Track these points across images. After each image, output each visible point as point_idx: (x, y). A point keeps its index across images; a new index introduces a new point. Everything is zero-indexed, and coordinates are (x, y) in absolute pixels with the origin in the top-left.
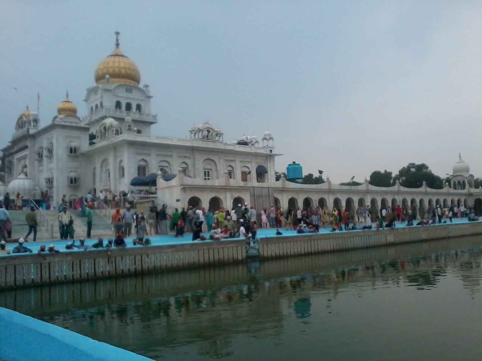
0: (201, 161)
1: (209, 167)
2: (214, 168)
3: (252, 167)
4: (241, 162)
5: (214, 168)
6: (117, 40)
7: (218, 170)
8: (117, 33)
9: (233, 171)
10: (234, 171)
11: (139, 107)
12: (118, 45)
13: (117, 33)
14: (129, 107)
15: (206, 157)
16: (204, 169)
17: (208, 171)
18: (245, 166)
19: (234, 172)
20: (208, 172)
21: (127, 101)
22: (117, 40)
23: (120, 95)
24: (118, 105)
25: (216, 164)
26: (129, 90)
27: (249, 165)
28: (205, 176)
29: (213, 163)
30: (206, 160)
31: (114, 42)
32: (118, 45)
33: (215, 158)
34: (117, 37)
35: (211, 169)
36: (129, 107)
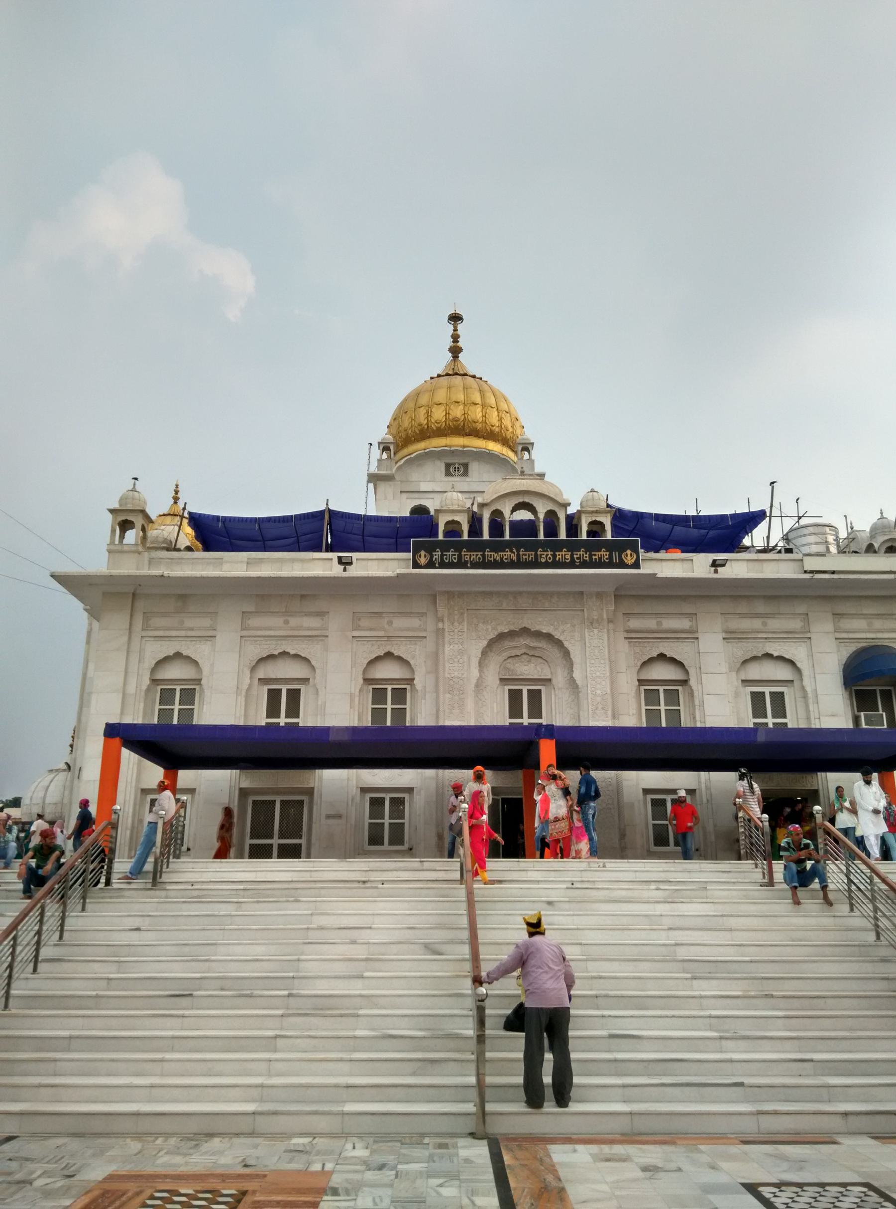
0: (476, 648)
3: (811, 655)
4: (731, 636)
5: (560, 679)
6: (455, 338)
7: (579, 682)
8: (455, 318)
9: (684, 682)
10: (693, 682)
12: (455, 351)
13: (455, 318)
16: (504, 681)
18: (768, 656)
19: (692, 694)
22: (455, 338)
23: (424, 487)
25: (566, 653)
27: (797, 652)
29: (554, 653)
30: (501, 637)
32: (455, 351)
34: (455, 330)
35: (550, 680)
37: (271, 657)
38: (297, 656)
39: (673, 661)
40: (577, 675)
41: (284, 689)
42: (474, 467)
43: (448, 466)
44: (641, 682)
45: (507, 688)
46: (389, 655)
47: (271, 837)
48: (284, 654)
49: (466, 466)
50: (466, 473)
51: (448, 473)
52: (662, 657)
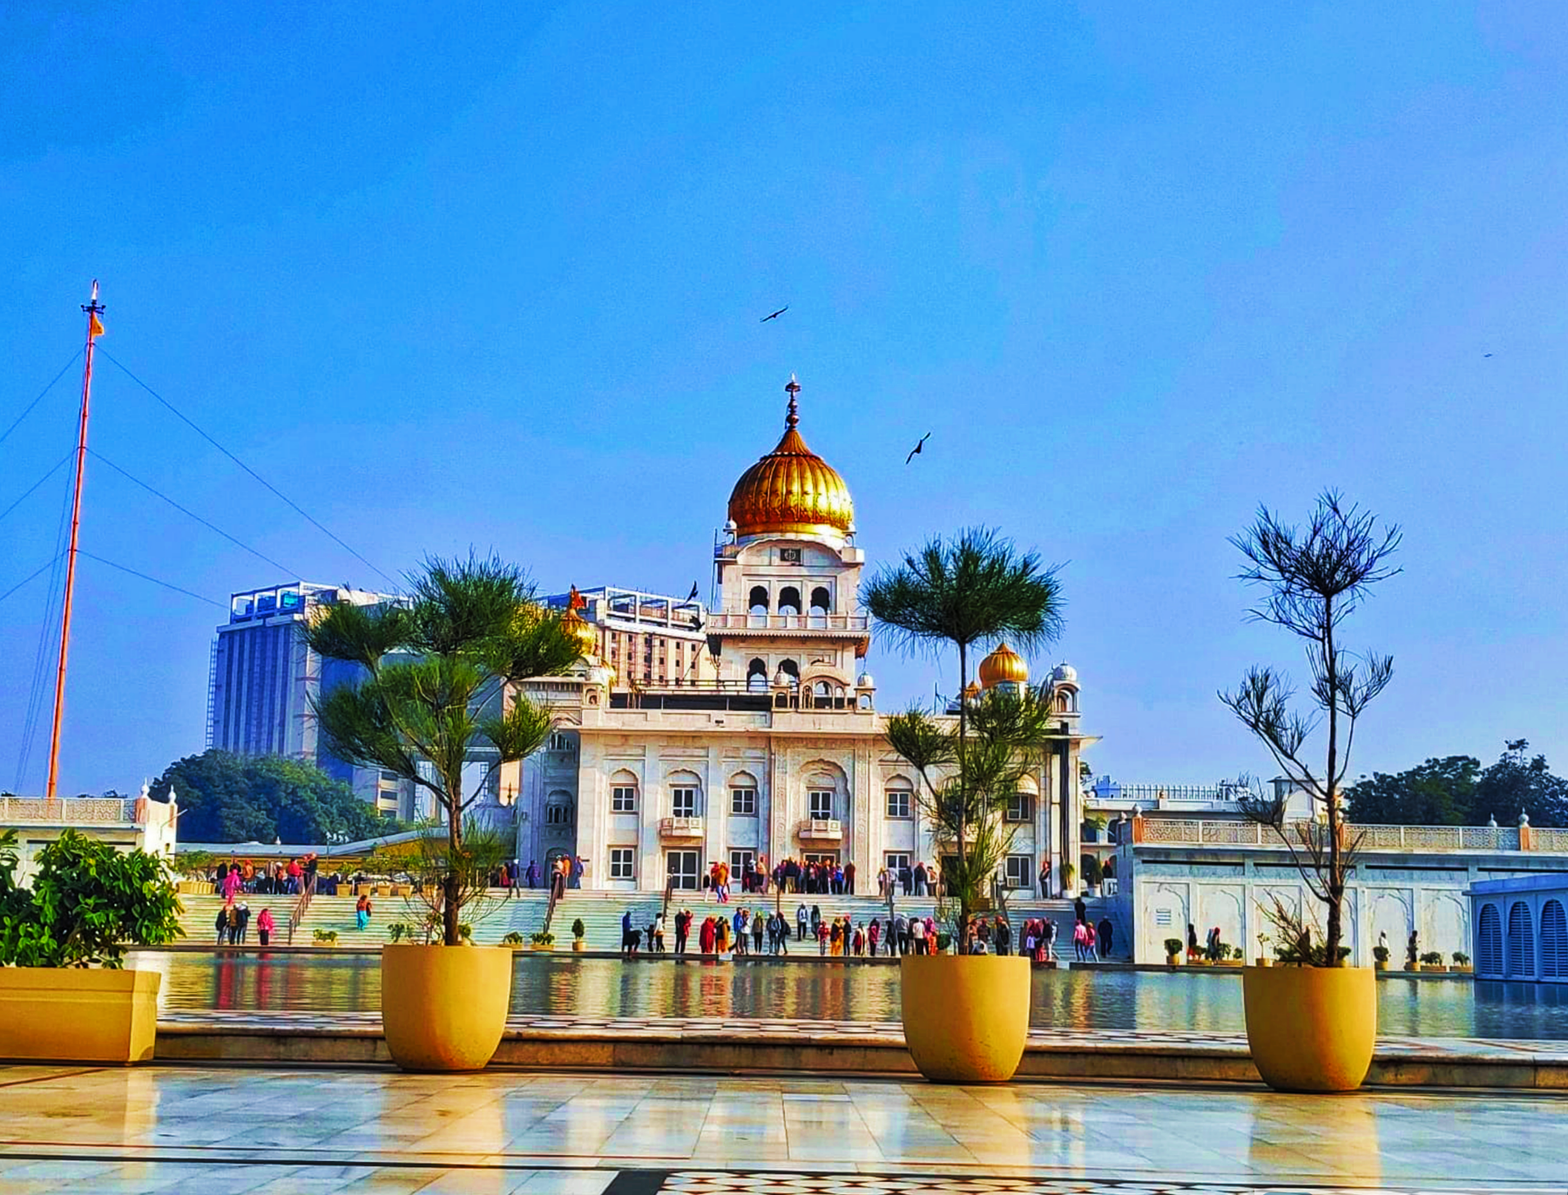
1: (826, 782)
2: (840, 788)
5: (840, 788)
6: (792, 407)
11: (822, 598)
12: (791, 420)
14: (790, 597)
15: (814, 754)
17: (823, 794)
20: (826, 797)
21: (787, 585)
22: (792, 407)
24: (758, 597)
26: (792, 554)
28: (815, 805)
29: (837, 774)
31: (785, 413)
32: (791, 420)
33: (841, 757)
36: (790, 597)
37: (676, 772)
38: (691, 772)
39: (905, 778)
40: (849, 787)
41: (683, 790)
42: (807, 555)
43: (783, 551)
44: (887, 790)
45: (811, 792)
46: (743, 772)
47: (684, 872)
48: (684, 770)
49: (798, 552)
50: (798, 559)
51: (783, 559)
52: (899, 776)
